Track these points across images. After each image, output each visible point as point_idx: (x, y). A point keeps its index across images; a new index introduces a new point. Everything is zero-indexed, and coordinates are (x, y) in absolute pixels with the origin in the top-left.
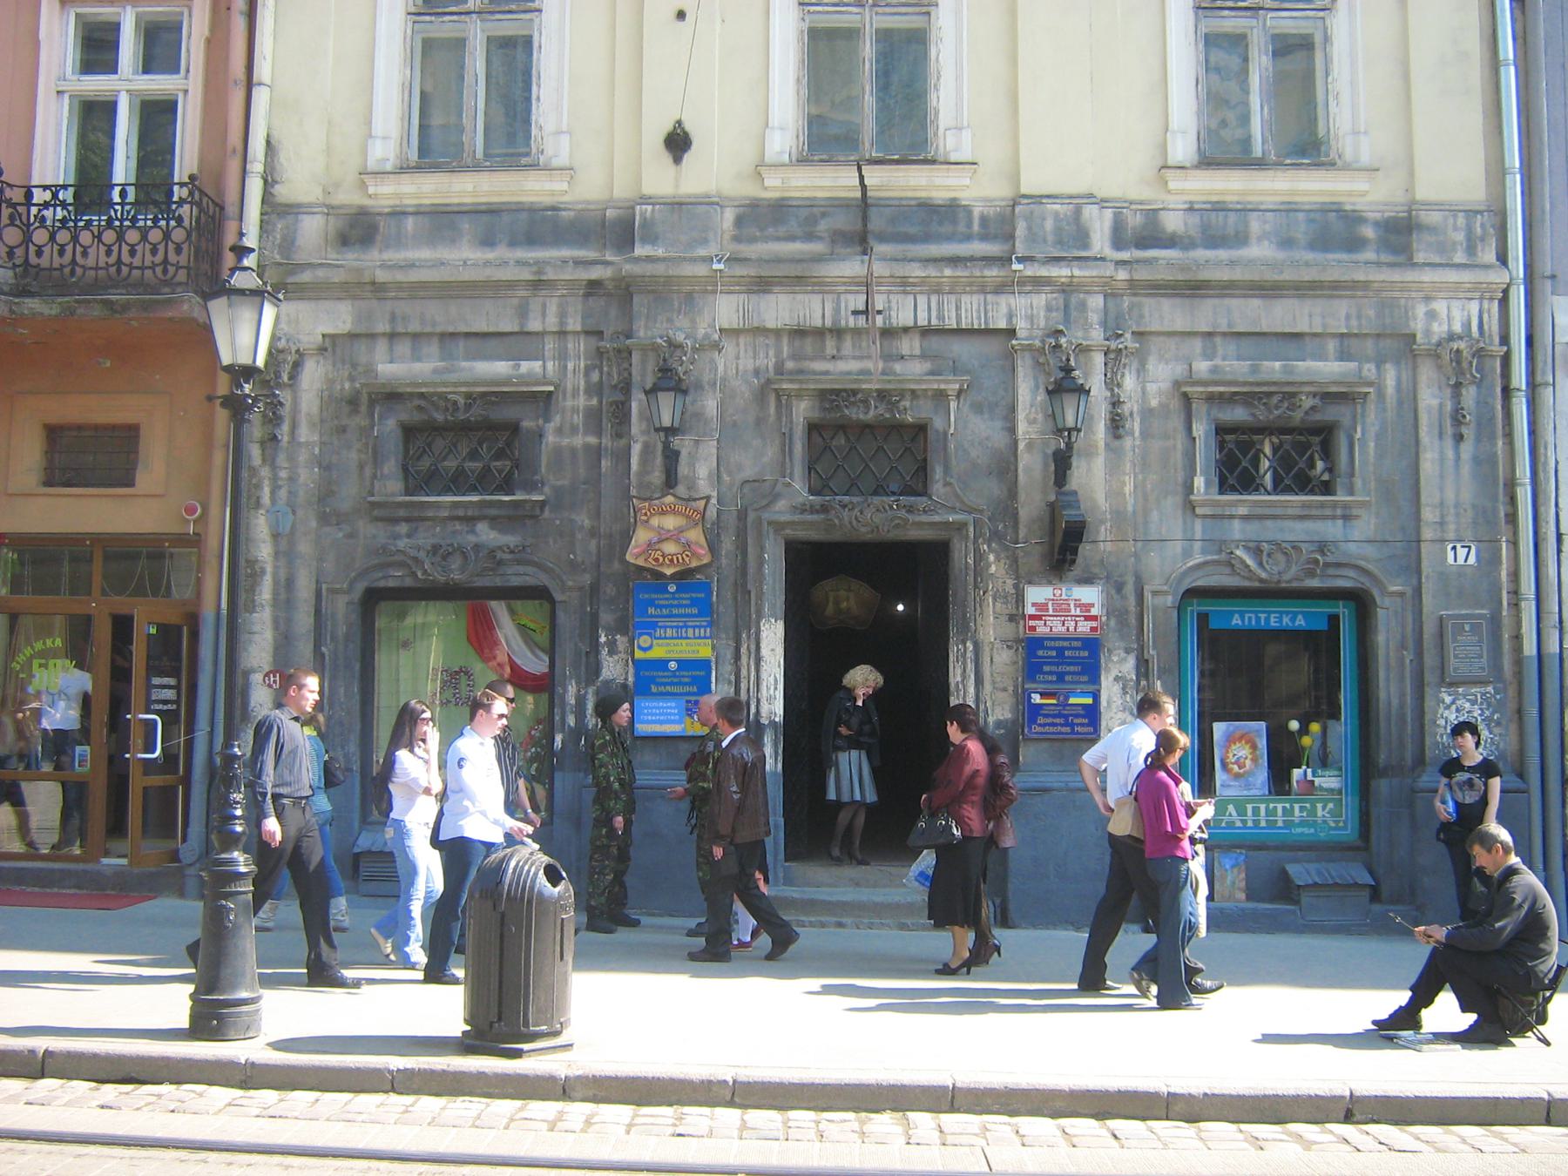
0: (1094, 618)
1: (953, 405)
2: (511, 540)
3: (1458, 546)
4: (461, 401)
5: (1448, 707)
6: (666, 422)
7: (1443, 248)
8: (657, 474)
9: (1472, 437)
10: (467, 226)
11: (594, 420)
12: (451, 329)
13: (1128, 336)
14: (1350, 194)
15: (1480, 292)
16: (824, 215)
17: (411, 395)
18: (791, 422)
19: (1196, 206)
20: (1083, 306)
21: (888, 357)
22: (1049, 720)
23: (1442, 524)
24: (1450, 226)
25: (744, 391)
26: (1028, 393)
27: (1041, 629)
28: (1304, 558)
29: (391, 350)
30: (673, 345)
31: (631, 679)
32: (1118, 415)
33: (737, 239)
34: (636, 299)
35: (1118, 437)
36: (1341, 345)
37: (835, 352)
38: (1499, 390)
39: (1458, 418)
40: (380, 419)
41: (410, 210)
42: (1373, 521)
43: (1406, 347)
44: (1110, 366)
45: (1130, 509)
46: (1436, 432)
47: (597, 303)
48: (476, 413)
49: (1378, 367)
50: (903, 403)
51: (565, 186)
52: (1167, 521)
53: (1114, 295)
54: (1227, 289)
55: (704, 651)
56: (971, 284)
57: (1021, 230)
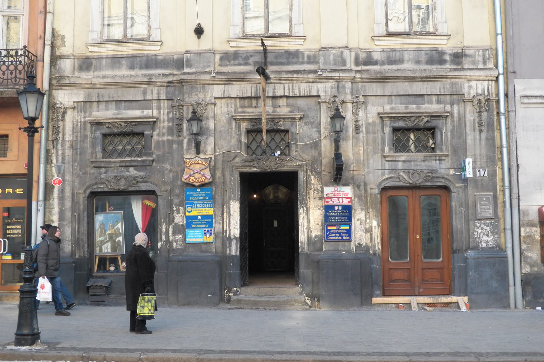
0: (349, 198)
1: (298, 123)
2: (142, 174)
3: (481, 170)
4: (123, 124)
5: (478, 228)
6: (195, 132)
7: (474, 63)
8: (193, 149)
9: (485, 130)
10: (124, 62)
11: (170, 131)
12: (119, 99)
13: (361, 97)
14: (440, 44)
15: (487, 78)
16: (251, 56)
17: (105, 122)
18: (241, 130)
19: (385, 50)
20: (344, 87)
21: (274, 106)
22: (334, 235)
24: (477, 55)
25: (223, 119)
26: (324, 117)
27: (330, 203)
28: (424, 175)
29: (98, 107)
31: (185, 223)
32: (357, 125)
33: (220, 65)
34: (185, 87)
35: (357, 133)
36: (438, 99)
37: (256, 105)
38: (495, 114)
39: (480, 125)
40: (94, 131)
41: (104, 57)
42: (450, 161)
44: (354, 108)
45: (362, 159)
46: (473, 129)
47: (171, 89)
48: (128, 129)
49: (451, 106)
50: (280, 123)
51: (159, 47)
52: (375, 162)
53: (355, 82)
54: (397, 79)
55: (210, 212)
56: (304, 80)
57: (321, 61)
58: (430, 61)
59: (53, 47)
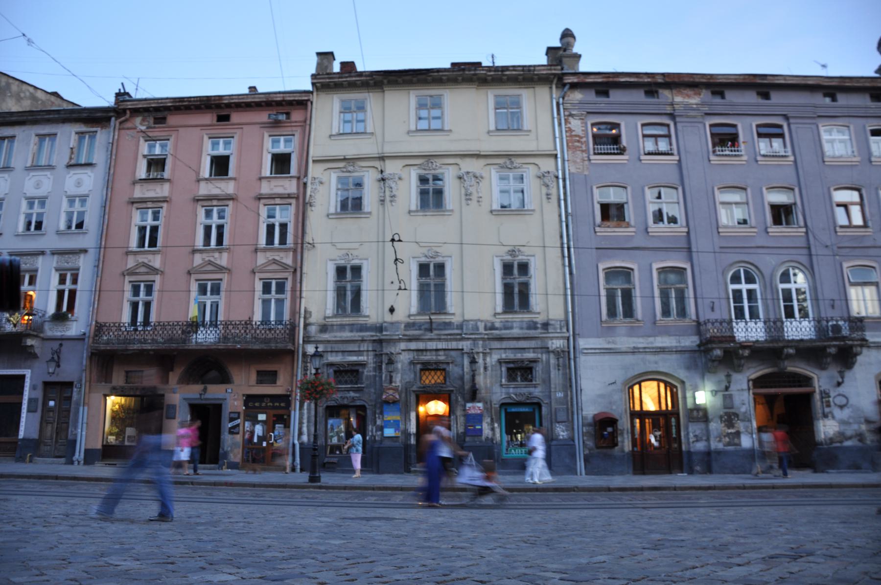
7: (555, 329)
11: (375, 369)
15: (562, 338)
20: (478, 344)
23: (556, 388)
25: (406, 362)
26: (466, 362)
27: (470, 412)
30: (392, 353)
33: (405, 330)
39: (558, 366)
43: (546, 350)
47: (375, 344)
52: (497, 389)
54: (509, 339)
55: (398, 418)
57: (464, 328)
58: (529, 328)
59: (305, 318)
